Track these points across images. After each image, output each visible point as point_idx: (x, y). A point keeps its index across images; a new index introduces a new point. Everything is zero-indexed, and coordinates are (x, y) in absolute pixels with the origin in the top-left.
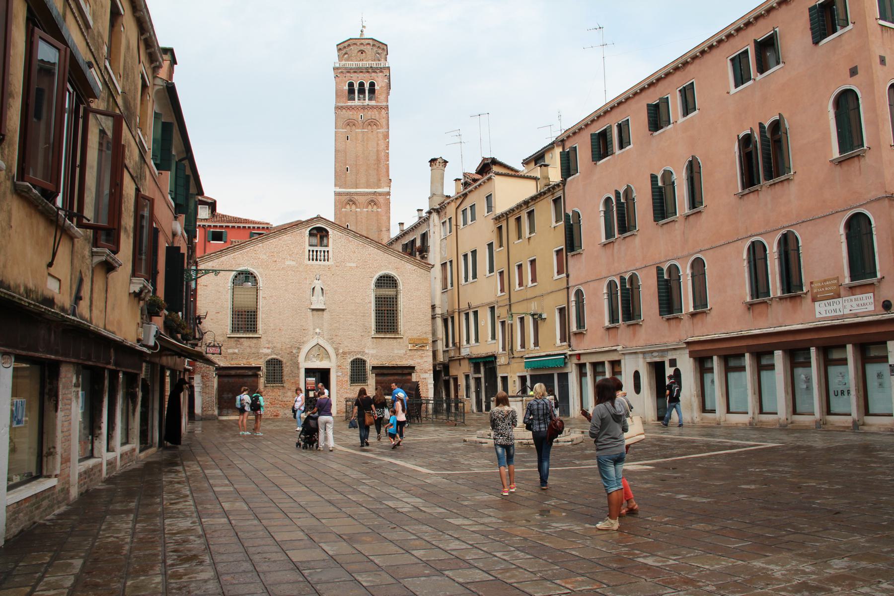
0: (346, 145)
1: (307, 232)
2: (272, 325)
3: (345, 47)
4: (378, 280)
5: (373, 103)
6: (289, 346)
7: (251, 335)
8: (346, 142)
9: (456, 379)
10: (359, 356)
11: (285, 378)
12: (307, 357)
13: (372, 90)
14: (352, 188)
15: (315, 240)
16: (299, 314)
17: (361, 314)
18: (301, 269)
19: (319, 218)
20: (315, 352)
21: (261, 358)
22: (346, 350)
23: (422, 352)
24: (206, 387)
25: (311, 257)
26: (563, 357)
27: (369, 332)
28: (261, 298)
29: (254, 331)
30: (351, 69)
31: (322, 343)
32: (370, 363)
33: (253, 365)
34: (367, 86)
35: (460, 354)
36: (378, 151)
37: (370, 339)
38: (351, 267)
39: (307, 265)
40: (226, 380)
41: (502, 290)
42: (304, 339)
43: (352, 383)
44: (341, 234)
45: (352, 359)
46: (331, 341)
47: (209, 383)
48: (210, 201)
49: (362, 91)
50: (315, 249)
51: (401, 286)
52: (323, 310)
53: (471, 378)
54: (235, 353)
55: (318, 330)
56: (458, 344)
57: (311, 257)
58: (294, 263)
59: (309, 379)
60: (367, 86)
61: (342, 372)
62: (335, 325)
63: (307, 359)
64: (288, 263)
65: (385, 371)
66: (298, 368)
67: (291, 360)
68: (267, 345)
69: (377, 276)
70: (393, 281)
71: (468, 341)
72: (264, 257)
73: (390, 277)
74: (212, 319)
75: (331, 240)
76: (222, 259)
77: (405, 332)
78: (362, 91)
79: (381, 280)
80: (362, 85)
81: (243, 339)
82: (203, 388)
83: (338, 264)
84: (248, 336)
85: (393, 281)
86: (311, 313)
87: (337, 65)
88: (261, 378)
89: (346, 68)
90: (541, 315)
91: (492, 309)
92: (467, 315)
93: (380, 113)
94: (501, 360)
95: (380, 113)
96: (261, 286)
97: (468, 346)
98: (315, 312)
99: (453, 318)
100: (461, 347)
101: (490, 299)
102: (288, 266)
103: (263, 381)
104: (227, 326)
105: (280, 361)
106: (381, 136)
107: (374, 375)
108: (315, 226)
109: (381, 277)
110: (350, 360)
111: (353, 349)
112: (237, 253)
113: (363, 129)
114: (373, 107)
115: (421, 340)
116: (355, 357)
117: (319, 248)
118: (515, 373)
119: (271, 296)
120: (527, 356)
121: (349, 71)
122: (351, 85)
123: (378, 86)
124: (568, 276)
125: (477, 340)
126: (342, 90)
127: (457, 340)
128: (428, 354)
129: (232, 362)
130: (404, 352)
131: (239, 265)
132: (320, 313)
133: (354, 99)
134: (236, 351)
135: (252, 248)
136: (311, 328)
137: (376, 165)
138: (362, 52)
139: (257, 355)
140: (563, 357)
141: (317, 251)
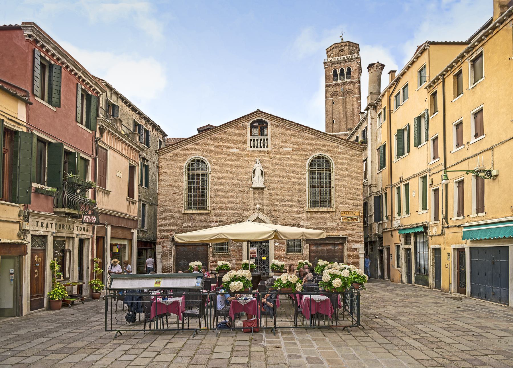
0: (332, 107)
1: (249, 125)
2: (219, 203)
5: (350, 80)
6: (233, 220)
7: (201, 212)
8: (332, 105)
9: (388, 249)
15: (256, 131)
16: (242, 193)
17: (297, 191)
18: (243, 155)
19: (258, 112)
23: (354, 224)
25: (252, 145)
27: (304, 207)
29: (204, 208)
30: (335, 62)
35: (392, 226)
36: (353, 108)
37: (305, 213)
38: (287, 152)
39: (249, 152)
42: (247, 214)
43: (288, 252)
44: (279, 124)
47: (168, 252)
49: (342, 74)
50: (256, 138)
52: (263, 189)
53: (401, 248)
54: (188, 226)
55: (258, 206)
56: (390, 217)
57: (252, 145)
61: (279, 242)
64: (234, 150)
68: (215, 220)
71: (399, 214)
72: (213, 146)
74: (170, 199)
75: (269, 130)
77: (337, 206)
78: (342, 74)
79: (315, 161)
80: (342, 70)
82: (162, 256)
83: (276, 149)
84: (199, 212)
87: (326, 61)
88: (211, 248)
89: (331, 62)
92: (399, 188)
93: (354, 86)
94: (434, 230)
95: (354, 86)
96: (210, 170)
97: (400, 218)
98: (256, 191)
99: (386, 194)
100: (393, 219)
102: (233, 153)
103: (212, 250)
104: (182, 204)
106: (355, 99)
107: (308, 245)
108: (256, 119)
113: (343, 96)
114: (349, 83)
117: (259, 137)
119: (219, 179)
120: (467, 224)
121: (333, 63)
122: (335, 71)
125: (408, 212)
127: (389, 214)
128: (359, 225)
130: (337, 224)
132: (261, 191)
134: (190, 225)
136: (252, 204)
141: (257, 140)
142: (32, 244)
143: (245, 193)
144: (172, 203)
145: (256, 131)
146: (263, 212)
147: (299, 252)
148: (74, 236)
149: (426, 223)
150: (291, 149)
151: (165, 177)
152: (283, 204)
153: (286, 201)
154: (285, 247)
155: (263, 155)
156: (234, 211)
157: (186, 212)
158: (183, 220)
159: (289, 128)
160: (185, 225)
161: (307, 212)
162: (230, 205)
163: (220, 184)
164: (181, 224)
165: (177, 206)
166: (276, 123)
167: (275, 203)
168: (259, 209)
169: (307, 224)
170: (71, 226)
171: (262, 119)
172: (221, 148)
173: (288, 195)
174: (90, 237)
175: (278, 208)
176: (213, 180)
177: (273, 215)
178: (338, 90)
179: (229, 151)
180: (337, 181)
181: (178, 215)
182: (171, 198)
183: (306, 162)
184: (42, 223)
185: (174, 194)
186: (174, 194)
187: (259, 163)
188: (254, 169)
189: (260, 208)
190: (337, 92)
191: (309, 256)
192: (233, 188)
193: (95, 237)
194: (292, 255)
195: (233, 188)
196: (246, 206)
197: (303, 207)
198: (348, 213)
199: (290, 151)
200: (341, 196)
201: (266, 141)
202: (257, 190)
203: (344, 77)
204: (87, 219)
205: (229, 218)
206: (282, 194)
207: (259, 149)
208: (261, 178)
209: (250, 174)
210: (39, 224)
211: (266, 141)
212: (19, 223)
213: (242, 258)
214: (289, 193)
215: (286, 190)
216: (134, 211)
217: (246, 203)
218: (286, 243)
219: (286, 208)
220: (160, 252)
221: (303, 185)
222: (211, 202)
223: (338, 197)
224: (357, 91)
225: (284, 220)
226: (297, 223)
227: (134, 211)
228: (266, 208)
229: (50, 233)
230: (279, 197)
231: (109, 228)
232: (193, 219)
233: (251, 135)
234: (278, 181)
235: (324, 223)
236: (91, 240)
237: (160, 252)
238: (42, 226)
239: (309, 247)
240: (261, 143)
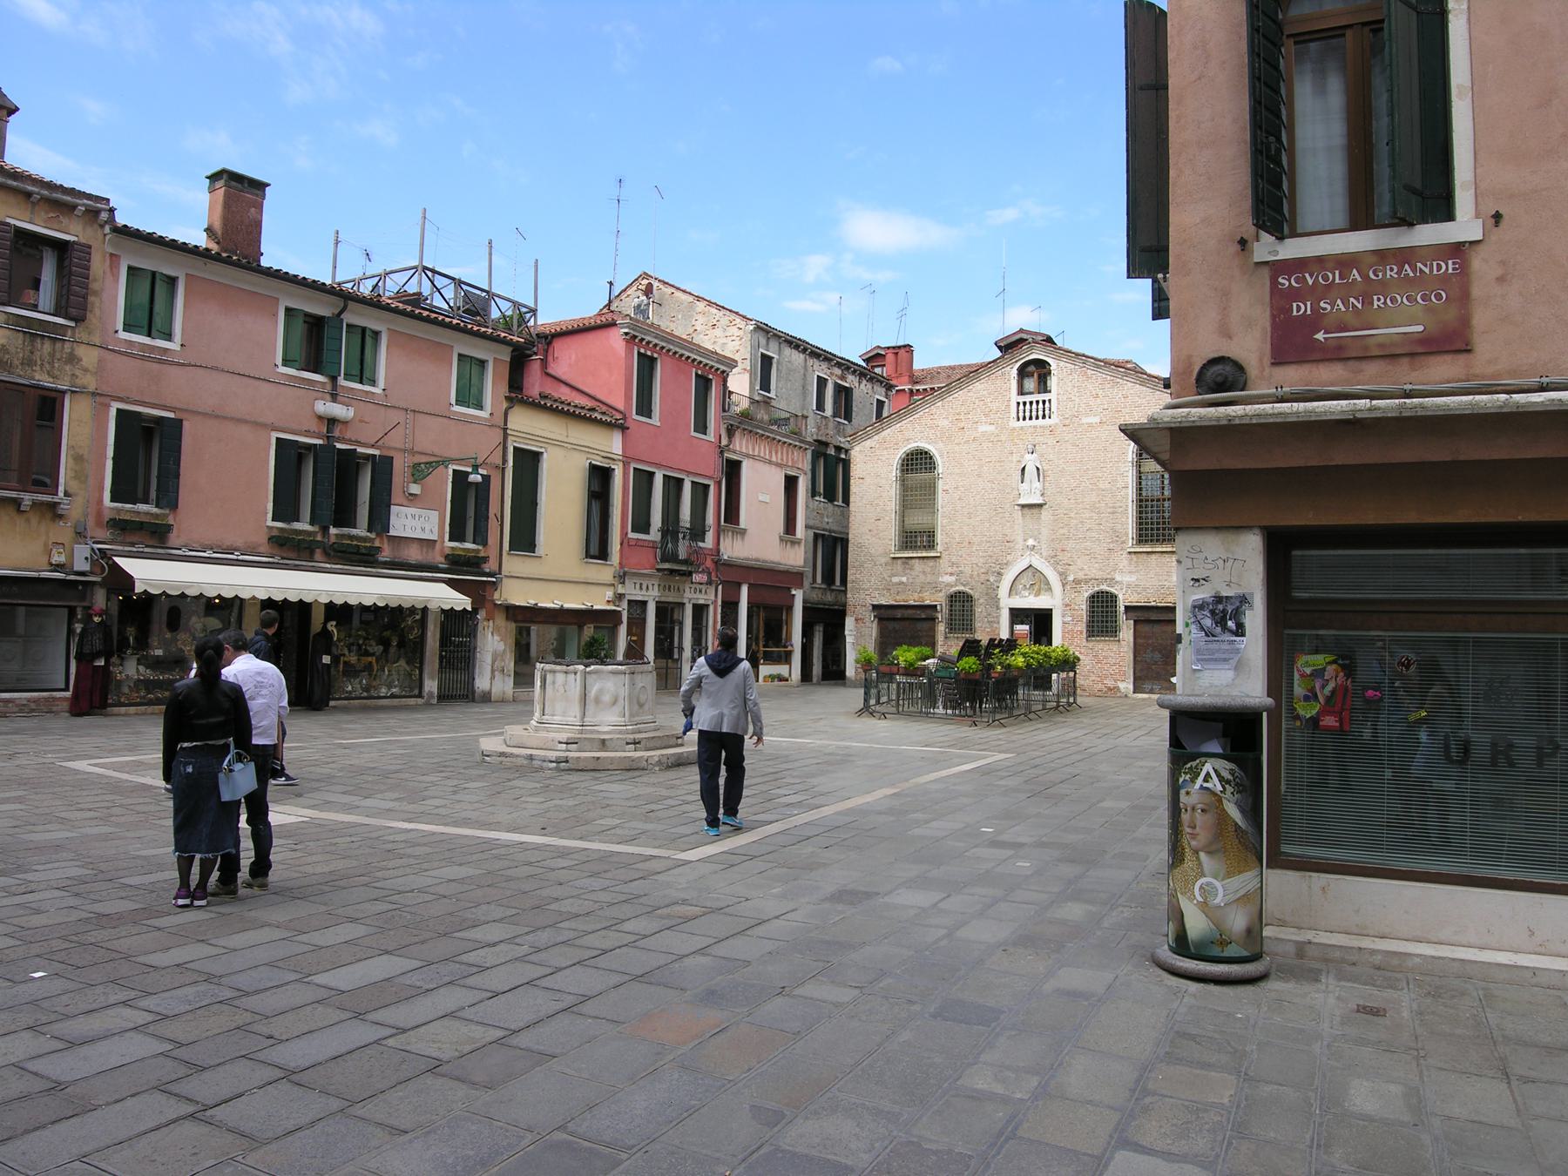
1: (1014, 372)
2: (957, 536)
6: (983, 570)
7: (924, 555)
10: (1104, 587)
11: (978, 625)
12: (1012, 590)
15: (1030, 384)
17: (1109, 510)
18: (1003, 438)
20: (1026, 580)
21: (941, 591)
22: (1081, 575)
24: (862, 636)
25: (1021, 415)
27: (1123, 542)
28: (940, 491)
31: (1038, 563)
32: (1124, 599)
33: (927, 602)
37: (1125, 555)
38: (1090, 425)
39: (1014, 429)
40: (891, 625)
44: (1073, 366)
45: (1091, 592)
46: (1053, 560)
47: (866, 631)
50: (1028, 398)
52: (1040, 506)
54: (901, 583)
55: (1031, 542)
57: (1021, 415)
61: (1072, 616)
62: (1062, 531)
63: (1014, 592)
64: (983, 428)
65: (1154, 617)
66: (998, 608)
67: (987, 594)
68: (950, 570)
72: (946, 423)
74: (870, 531)
76: (883, 433)
81: (913, 561)
82: (857, 638)
83: (1067, 422)
84: (920, 555)
86: (1020, 513)
96: (940, 471)
98: (1026, 511)
102: (983, 434)
103: (943, 628)
104: (891, 540)
107: (1132, 622)
108: (1027, 359)
110: (1086, 595)
111: (1094, 572)
112: (905, 422)
116: (1096, 589)
117: (1034, 398)
131: (908, 440)
132: (1035, 511)
134: (904, 579)
135: (927, 410)
136: (1020, 539)
139: (934, 585)
141: (1031, 403)
142: (628, 611)
143: (1007, 515)
144: (874, 539)
145: (1030, 384)
147: (1112, 636)
148: (685, 601)
150: (1096, 420)
154: (1084, 625)
157: (897, 556)
159: (1093, 372)
160: (895, 580)
161: (1130, 553)
164: (888, 579)
166: (1068, 365)
169: (1129, 579)
170: (681, 589)
172: (962, 425)
173: (1091, 518)
174: (710, 602)
175: (1070, 545)
181: (883, 560)
184: (641, 584)
187: (1032, 453)
189: (1034, 546)
191: (1132, 644)
193: (720, 603)
194: (1098, 641)
205: (974, 566)
208: (1037, 485)
210: (638, 586)
211: (1047, 404)
212: (613, 585)
214: (1094, 514)
215: (1088, 507)
216: (795, 557)
217: (1007, 535)
218: (1085, 617)
222: (942, 535)
225: (1082, 569)
226: (1109, 577)
227: (795, 557)
228: (1045, 546)
229: (652, 598)
231: (744, 590)
233: (1021, 392)
235: (1167, 578)
236: (711, 608)
238: (641, 588)
239: (1132, 627)
240: (1037, 409)
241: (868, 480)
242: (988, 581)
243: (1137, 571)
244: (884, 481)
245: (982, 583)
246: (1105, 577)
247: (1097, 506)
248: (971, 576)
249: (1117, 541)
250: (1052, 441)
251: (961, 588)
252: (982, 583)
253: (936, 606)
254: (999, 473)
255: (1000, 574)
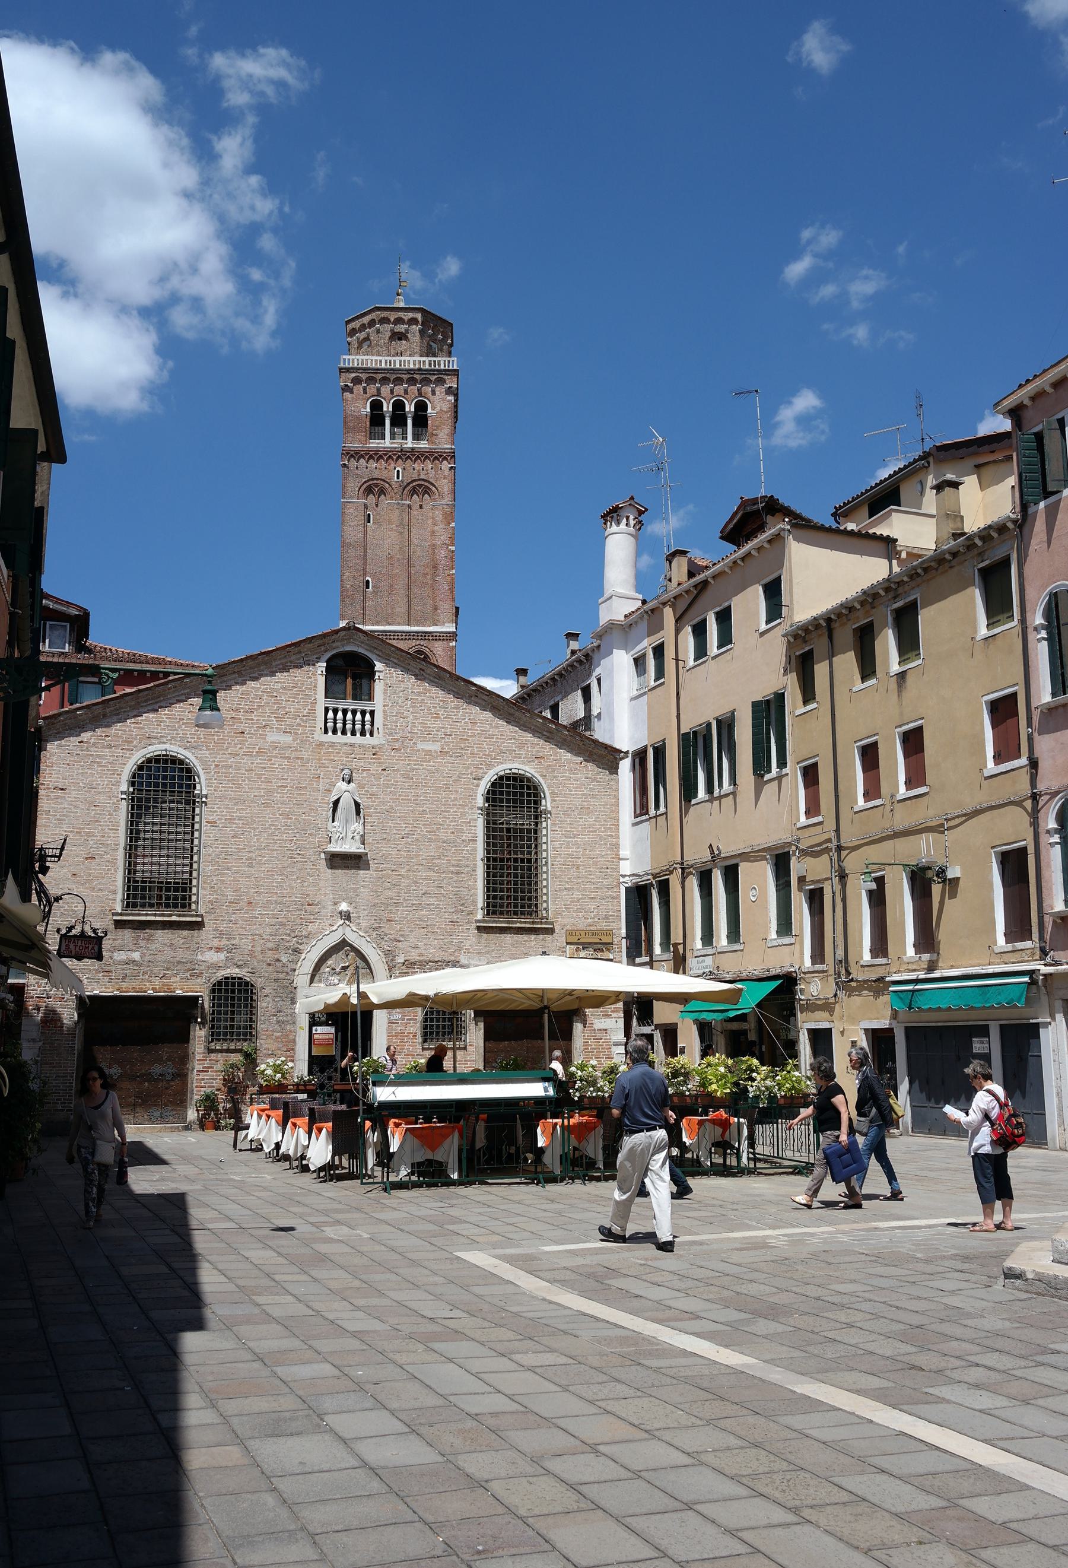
0: (365, 532)
2: (229, 892)
3: (363, 327)
4: (493, 784)
5: (423, 445)
6: (270, 945)
8: (365, 526)
13: (421, 420)
14: (378, 623)
16: (299, 865)
18: (305, 755)
21: (200, 975)
22: (414, 956)
25: (330, 725)
26: (1026, 979)
27: (470, 913)
29: (183, 906)
31: (352, 938)
33: (179, 992)
34: (410, 408)
38: (428, 753)
41: (813, 809)
46: (376, 932)
48: (74, 612)
51: (547, 804)
55: (344, 907)
57: (330, 725)
58: (287, 739)
59: (320, 1029)
60: (410, 408)
63: (317, 978)
64: (272, 737)
68: (216, 943)
69: (490, 776)
70: (529, 788)
71: (708, 937)
73: (522, 781)
77: (558, 913)
79: (501, 786)
80: (399, 406)
83: (397, 745)
85: (529, 788)
90: (944, 871)
91: (781, 863)
94: (812, 989)
101: (777, 835)
102: (275, 745)
105: (247, 984)
106: (439, 515)
109: (501, 778)
115: (595, 934)
118: (854, 1020)
119: (230, 820)
122: (376, 406)
123: (433, 409)
124: (1034, 764)
126: (358, 418)
127: (676, 936)
129: (124, 985)
133: (382, 437)
134: (136, 956)
136: (328, 901)
137: (429, 577)
138: (401, 336)
139: (188, 966)
140: (1026, 979)
146: (359, 924)
149: (793, 970)
151: (62, 804)
152: (413, 904)
153: (423, 894)
154: (418, 1025)
155: (360, 759)
156: (274, 918)
158: (114, 940)
162: (260, 899)
163: (233, 837)
165: (98, 896)
167: (392, 899)
168: (347, 916)
171: (361, 650)
172: (241, 728)
176: (212, 823)
177: (386, 935)
178: (384, 474)
179: (263, 737)
180: (557, 844)
182: (77, 871)
183: (478, 786)
185: (87, 858)
186: (87, 858)
188: (336, 798)
190: (382, 483)
192: (274, 850)
195: (274, 850)
196: (309, 905)
197: (468, 914)
198: (583, 936)
199: (436, 752)
200: (567, 886)
201: (368, 717)
202: (341, 859)
203: (405, 433)
204: (72, 946)
206: (410, 874)
207: (349, 738)
209: (323, 810)
211: (368, 717)
213: (293, 1057)
217: (308, 895)
219: (423, 915)
220: (34, 1040)
221: (467, 850)
223: (560, 890)
224: (446, 489)
225: (416, 947)
226: (452, 958)
228: (366, 913)
230: (405, 882)
232: (148, 940)
234: (401, 836)
237: (34, 1040)
240: (354, 721)
241: (72, 794)
242: (278, 960)
243: (488, 952)
244: (102, 798)
245: (269, 965)
246: (447, 959)
247: (437, 861)
248: (251, 954)
249: (463, 911)
250: (375, 768)
251: (234, 972)
252: (269, 965)
253: (197, 998)
254: (299, 804)
255: (297, 951)
